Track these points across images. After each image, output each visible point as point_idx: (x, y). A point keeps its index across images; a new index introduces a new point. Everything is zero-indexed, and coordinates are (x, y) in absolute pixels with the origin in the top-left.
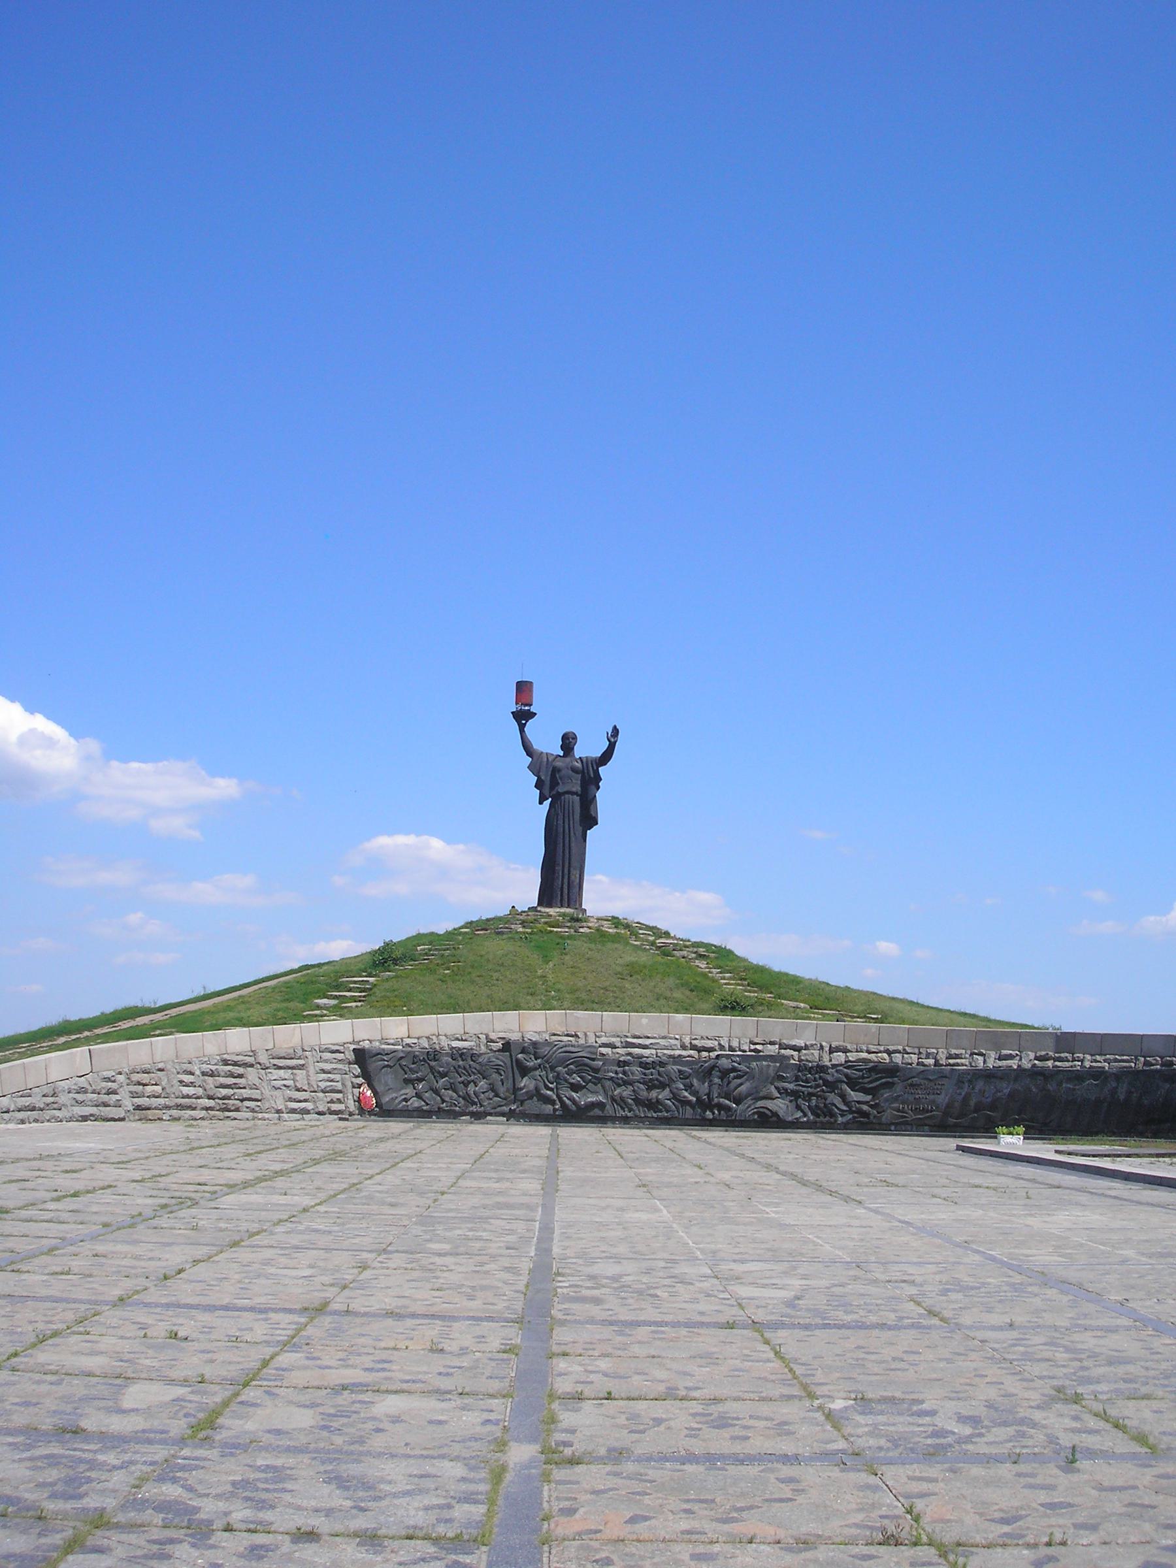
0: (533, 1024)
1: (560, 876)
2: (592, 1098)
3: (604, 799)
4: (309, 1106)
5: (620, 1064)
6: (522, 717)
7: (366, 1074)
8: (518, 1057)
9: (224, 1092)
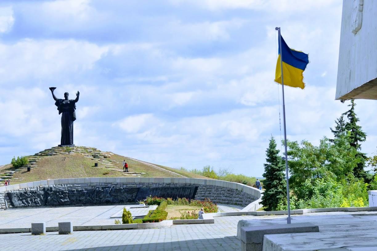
6: (52, 89)
8: (47, 192)
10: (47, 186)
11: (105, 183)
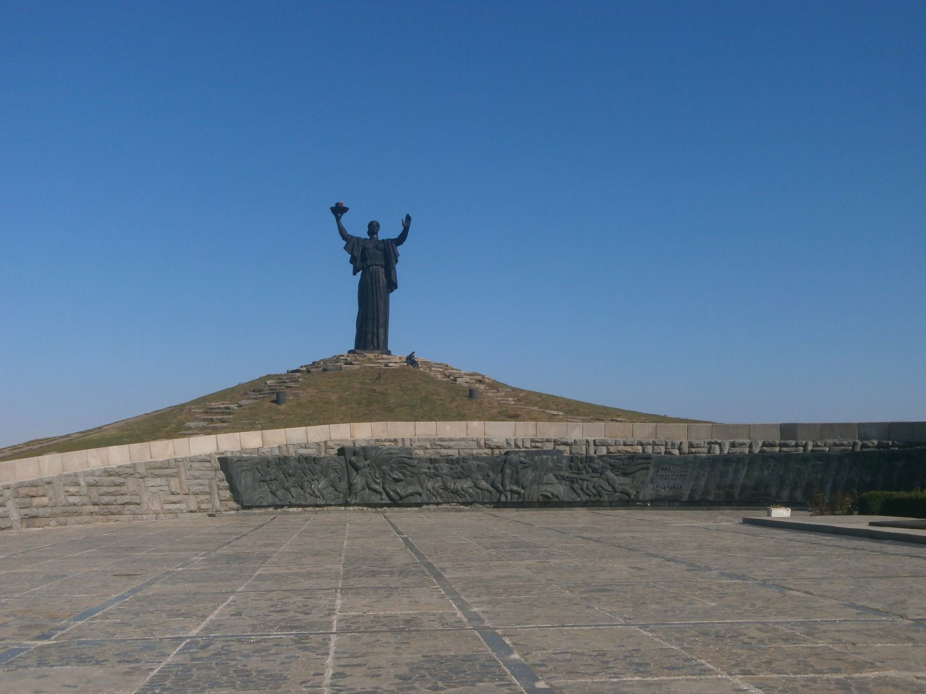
0: (363, 433)
1: (371, 328)
2: (411, 490)
3: (402, 270)
4: (182, 506)
5: (432, 461)
6: (339, 210)
7: (229, 478)
8: (350, 457)
9: (106, 499)
10: (350, 444)
11: (533, 441)
